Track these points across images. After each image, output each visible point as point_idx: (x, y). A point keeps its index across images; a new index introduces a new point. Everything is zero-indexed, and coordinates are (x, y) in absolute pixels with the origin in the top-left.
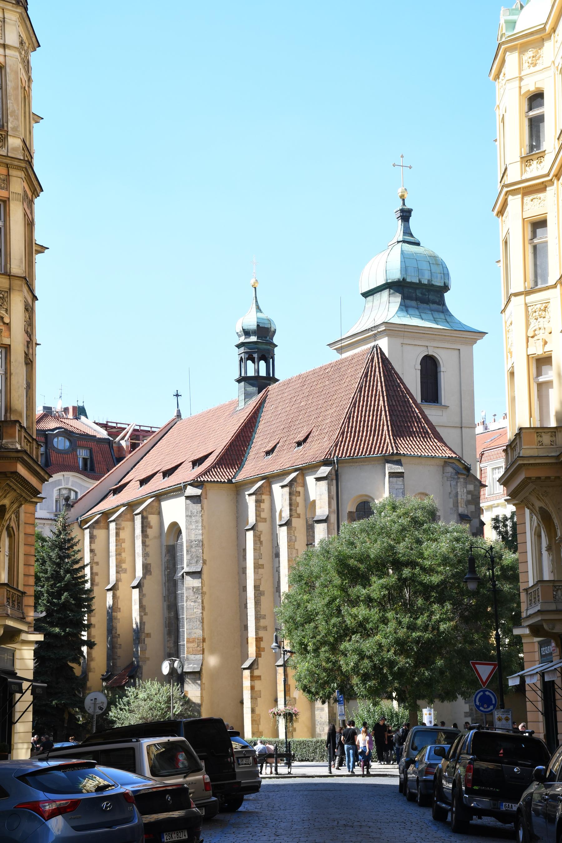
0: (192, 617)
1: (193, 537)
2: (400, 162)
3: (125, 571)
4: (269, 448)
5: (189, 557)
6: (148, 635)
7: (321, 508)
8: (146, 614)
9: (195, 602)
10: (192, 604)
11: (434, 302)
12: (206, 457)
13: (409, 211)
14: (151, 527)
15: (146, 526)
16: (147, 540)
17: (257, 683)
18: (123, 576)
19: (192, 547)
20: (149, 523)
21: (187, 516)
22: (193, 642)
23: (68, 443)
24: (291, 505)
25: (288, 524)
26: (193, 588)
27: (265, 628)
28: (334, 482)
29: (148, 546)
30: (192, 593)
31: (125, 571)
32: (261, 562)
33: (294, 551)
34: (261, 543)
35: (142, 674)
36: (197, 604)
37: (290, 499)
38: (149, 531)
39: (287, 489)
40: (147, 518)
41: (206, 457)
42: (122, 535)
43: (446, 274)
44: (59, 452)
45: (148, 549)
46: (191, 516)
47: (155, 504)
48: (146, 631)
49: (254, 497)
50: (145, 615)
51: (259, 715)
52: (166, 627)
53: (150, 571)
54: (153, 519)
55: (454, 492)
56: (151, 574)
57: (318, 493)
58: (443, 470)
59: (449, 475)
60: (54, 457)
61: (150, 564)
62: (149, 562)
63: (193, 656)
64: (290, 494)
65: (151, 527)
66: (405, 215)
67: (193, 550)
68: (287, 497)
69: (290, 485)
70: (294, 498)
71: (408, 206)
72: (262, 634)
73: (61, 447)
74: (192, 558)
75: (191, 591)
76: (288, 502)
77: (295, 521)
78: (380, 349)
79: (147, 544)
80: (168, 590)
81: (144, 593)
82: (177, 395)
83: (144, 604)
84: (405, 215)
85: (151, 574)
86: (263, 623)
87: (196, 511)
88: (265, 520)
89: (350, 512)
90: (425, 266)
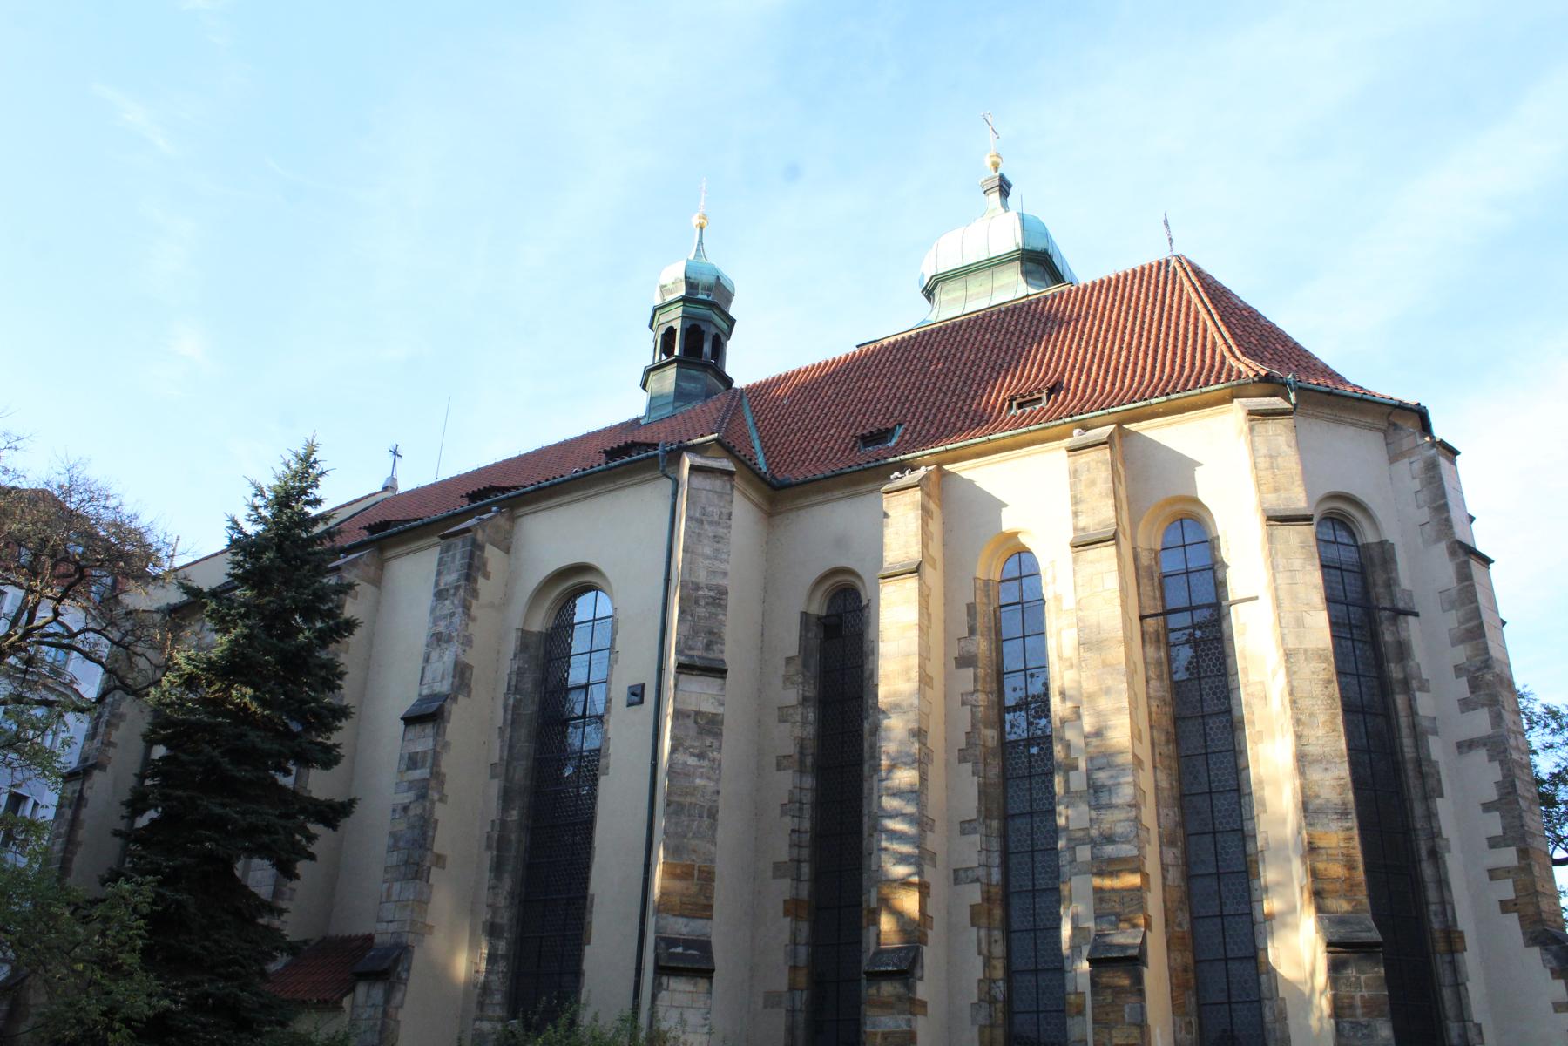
0: (688, 800)
1: (701, 577)
5: (686, 629)
6: (440, 860)
8: (442, 799)
9: (701, 756)
10: (692, 761)
14: (487, 576)
15: (478, 569)
16: (474, 602)
17: (921, 1025)
19: (696, 602)
20: (485, 565)
26: (698, 713)
29: (474, 620)
30: (693, 730)
34: (929, 615)
35: (408, 970)
36: (705, 763)
40: (482, 548)
46: (701, 522)
47: (502, 521)
48: (438, 848)
50: (441, 800)
52: (489, 847)
53: (468, 686)
54: (492, 554)
56: (469, 696)
57: (1263, 450)
61: (471, 667)
63: (681, 921)
65: (487, 576)
67: (701, 612)
74: (695, 632)
75: (690, 722)
78: (1189, 263)
79: (474, 611)
80: (511, 748)
81: (448, 738)
82: (395, 453)
83: (443, 769)
85: (469, 696)
87: (717, 511)
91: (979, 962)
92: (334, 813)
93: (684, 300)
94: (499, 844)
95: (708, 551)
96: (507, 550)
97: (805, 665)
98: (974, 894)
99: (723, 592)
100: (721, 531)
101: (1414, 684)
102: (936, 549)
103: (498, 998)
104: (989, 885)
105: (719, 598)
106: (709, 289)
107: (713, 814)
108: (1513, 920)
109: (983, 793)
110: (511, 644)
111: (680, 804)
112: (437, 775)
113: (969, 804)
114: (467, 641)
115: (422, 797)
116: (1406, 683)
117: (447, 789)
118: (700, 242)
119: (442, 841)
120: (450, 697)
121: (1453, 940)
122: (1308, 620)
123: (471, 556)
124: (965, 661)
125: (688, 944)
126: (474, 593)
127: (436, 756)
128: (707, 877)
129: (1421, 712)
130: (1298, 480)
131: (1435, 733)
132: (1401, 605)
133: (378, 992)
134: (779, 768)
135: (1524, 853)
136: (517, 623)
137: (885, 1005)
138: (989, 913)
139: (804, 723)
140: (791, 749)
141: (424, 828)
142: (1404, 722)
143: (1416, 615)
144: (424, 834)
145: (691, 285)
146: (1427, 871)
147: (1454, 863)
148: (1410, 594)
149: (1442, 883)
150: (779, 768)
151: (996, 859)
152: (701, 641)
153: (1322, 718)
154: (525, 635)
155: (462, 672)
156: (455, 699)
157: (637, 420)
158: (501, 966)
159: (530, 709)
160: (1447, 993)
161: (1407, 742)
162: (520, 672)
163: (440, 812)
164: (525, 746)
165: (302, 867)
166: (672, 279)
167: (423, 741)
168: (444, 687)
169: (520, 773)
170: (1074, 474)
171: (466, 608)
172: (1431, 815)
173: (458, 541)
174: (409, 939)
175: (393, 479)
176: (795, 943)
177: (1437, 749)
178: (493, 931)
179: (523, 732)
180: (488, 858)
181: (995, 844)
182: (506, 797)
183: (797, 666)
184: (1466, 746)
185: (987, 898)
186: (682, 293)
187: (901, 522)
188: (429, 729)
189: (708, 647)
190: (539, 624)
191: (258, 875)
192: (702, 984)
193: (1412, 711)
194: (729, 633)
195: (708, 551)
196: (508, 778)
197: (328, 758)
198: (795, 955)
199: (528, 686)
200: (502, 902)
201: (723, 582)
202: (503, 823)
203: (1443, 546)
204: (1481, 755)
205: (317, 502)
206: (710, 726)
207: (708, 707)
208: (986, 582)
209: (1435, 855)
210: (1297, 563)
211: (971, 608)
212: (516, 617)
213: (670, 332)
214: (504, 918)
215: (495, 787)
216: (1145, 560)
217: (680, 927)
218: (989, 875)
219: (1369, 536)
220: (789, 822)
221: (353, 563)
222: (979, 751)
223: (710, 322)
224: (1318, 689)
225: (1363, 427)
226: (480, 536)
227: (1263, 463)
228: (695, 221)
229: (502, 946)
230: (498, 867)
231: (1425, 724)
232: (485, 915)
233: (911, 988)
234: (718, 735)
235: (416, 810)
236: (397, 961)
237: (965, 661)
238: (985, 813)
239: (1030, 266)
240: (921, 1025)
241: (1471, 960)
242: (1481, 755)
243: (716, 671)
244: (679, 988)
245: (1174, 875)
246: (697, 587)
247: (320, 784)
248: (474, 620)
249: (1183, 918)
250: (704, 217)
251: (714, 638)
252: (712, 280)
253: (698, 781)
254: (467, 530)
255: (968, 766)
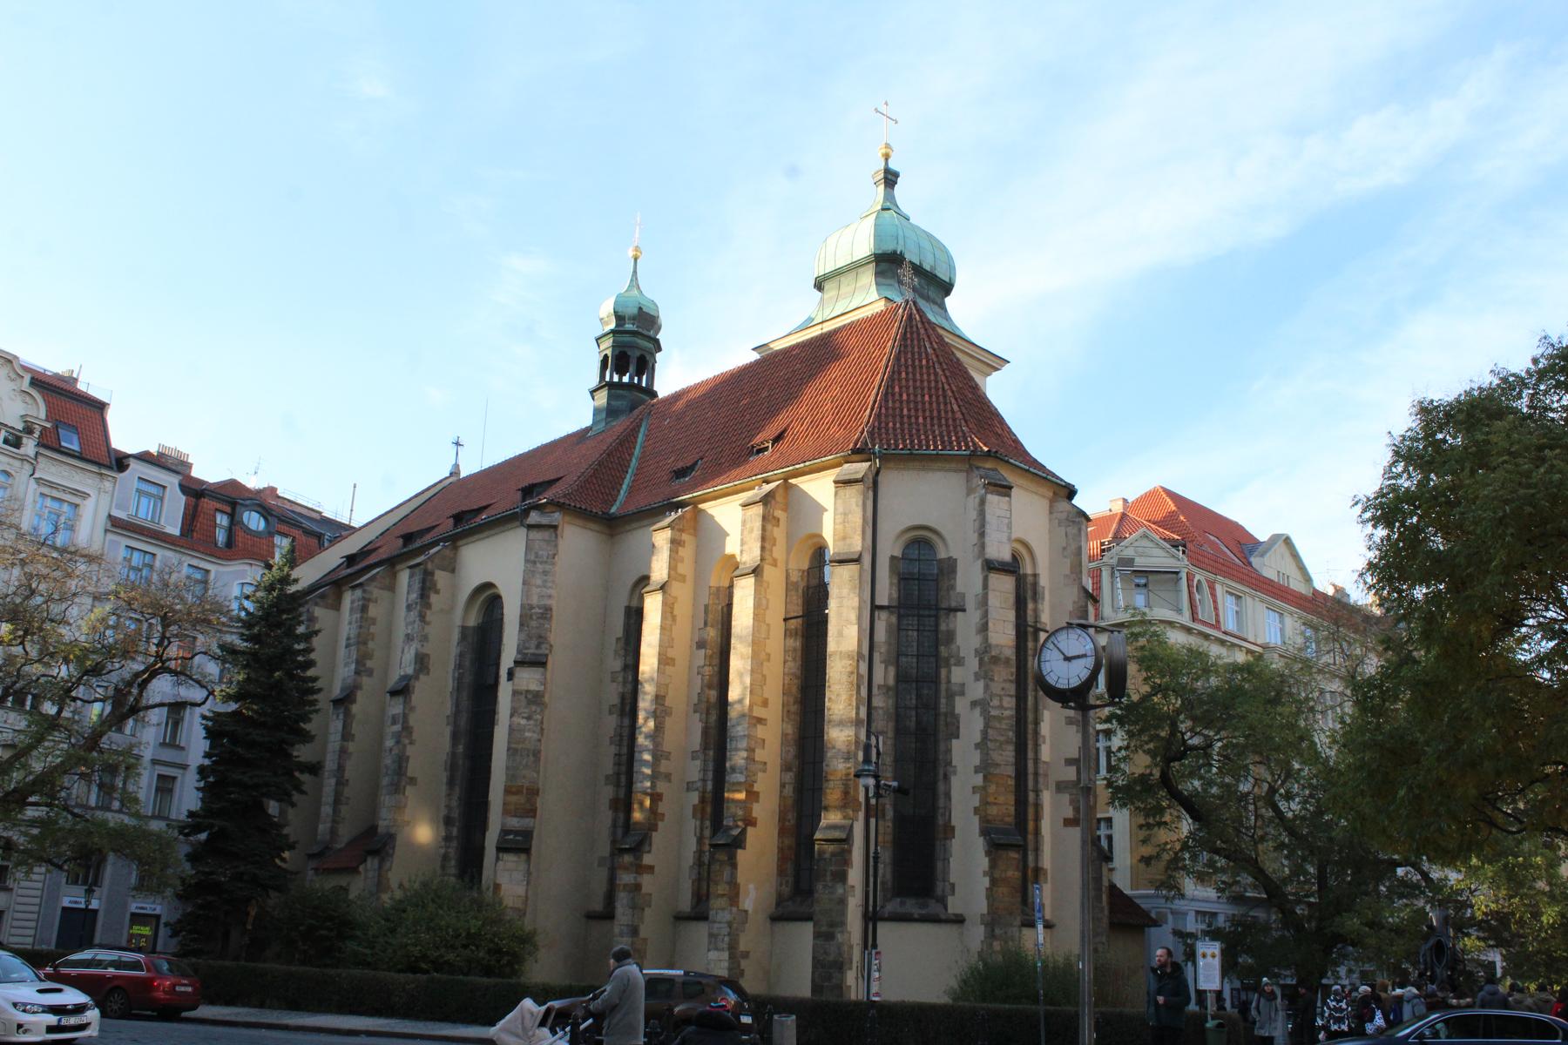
1: (535, 601)
2: (883, 109)
3: (370, 673)
4: (680, 465)
6: (413, 781)
7: (844, 538)
9: (529, 718)
10: (523, 722)
11: (935, 303)
12: (551, 483)
13: (896, 175)
14: (437, 592)
17: (646, 881)
18: (365, 680)
21: (527, 561)
22: (518, 792)
23: (262, 524)
24: (763, 539)
25: (756, 571)
27: (668, 777)
28: (871, 494)
29: (428, 623)
31: (370, 673)
32: (671, 653)
33: (764, 627)
34: (674, 618)
37: (764, 529)
38: (434, 598)
39: (758, 510)
40: (432, 574)
41: (551, 483)
42: (373, 611)
43: (951, 268)
44: (247, 530)
45: (427, 629)
47: (447, 552)
48: (409, 774)
49: (668, 533)
51: (645, 940)
54: (441, 577)
55: (1073, 547)
57: (841, 510)
58: (1051, 507)
59: (1064, 516)
60: (240, 537)
62: (425, 651)
64: (764, 518)
65: (437, 592)
66: (890, 179)
67: (534, 624)
68: (758, 524)
69: (766, 500)
70: (769, 527)
71: (893, 166)
72: (662, 787)
73: (253, 526)
74: (530, 637)
75: (522, 698)
76: (757, 533)
77: (768, 571)
79: (429, 616)
82: (457, 444)
83: (412, 722)
84: (890, 179)
86: (664, 766)
88: (683, 579)
89: (893, 558)
90: (926, 245)
91: (694, 841)
92: (314, 769)
93: (612, 331)
94: (452, 767)
95: (539, 582)
96: (453, 571)
97: (627, 643)
98: (694, 798)
99: (548, 609)
100: (548, 567)
101: (952, 661)
102: (685, 568)
103: (453, 863)
104: (704, 792)
105: (547, 611)
106: (633, 319)
107: (536, 754)
108: (976, 819)
109: (705, 732)
110: (456, 636)
111: (516, 750)
112: (407, 729)
113: (696, 740)
114: (425, 638)
115: (398, 742)
116: (947, 660)
117: (415, 736)
118: (635, 272)
119: (412, 769)
120: (416, 676)
121: (950, 831)
122: (846, 632)
123: (424, 581)
124: (701, 645)
125: (516, 833)
126: (428, 606)
127: (405, 716)
128: (534, 792)
129: (954, 680)
130: (859, 531)
131: (962, 694)
132: (953, 604)
133: (376, 861)
134: (611, 713)
135: (985, 777)
136: (458, 622)
137: (626, 869)
138: (703, 810)
139: (625, 682)
140: (616, 700)
141: (401, 761)
142: (943, 687)
143: (964, 610)
144: (400, 767)
145: (620, 318)
146: (941, 787)
147: (955, 782)
148: (963, 596)
149: (948, 796)
150: (611, 713)
151: (710, 775)
152: (533, 643)
153: (844, 697)
154: (464, 629)
155: (422, 662)
156: (417, 678)
157: (588, 429)
158: (454, 844)
159: (468, 679)
160: (939, 865)
161: (943, 701)
162: (461, 655)
163: (410, 751)
164: (465, 702)
165: (296, 797)
166: (603, 315)
167: (396, 707)
168: (410, 671)
169: (463, 721)
170: (744, 523)
171: (422, 617)
172: (949, 751)
173: (417, 570)
174: (393, 831)
175: (456, 466)
176: (614, 825)
177: (961, 705)
178: (448, 821)
179: (465, 695)
180: (444, 776)
181: (711, 766)
182: (455, 737)
183: (621, 644)
184: (974, 704)
185: (703, 800)
186: (612, 326)
187: (660, 549)
188: (401, 699)
189: (538, 647)
190: (472, 622)
191: (273, 807)
192: (523, 857)
193: (949, 681)
194: (553, 638)
195: (539, 582)
196: (456, 725)
197: (306, 737)
198: (614, 833)
199: (467, 663)
200: (454, 803)
201: (548, 602)
202: (453, 754)
203: (979, 562)
204: (977, 711)
205: (296, 581)
206: (535, 699)
207: (534, 687)
208: (718, 589)
209: (946, 778)
210: (845, 592)
211: (706, 607)
212: (458, 618)
213: (606, 357)
214: (455, 814)
215: (448, 731)
216: (795, 577)
217: (514, 823)
218: (705, 786)
219: (942, 555)
220: (613, 750)
221: (373, 579)
222: (704, 706)
223: (636, 347)
224: (844, 678)
225: (949, 470)
226: (430, 566)
227: (839, 520)
228: (631, 253)
229: (455, 831)
230: (451, 783)
231: (955, 688)
232: (443, 812)
233: (639, 858)
234: (543, 705)
235: (395, 751)
236: (385, 844)
237: (701, 645)
238: (705, 746)
239: (884, 266)
240: (646, 881)
241: (956, 845)
242: (977, 711)
243: (539, 662)
244: (510, 859)
245: (789, 790)
246: (532, 607)
247: (303, 753)
248: (428, 623)
249: (791, 816)
250: (637, 249)
251: (541, 639)
252: (635, 311)
253: (527, 734)
254: (418, 565)
255: (697, 715)
